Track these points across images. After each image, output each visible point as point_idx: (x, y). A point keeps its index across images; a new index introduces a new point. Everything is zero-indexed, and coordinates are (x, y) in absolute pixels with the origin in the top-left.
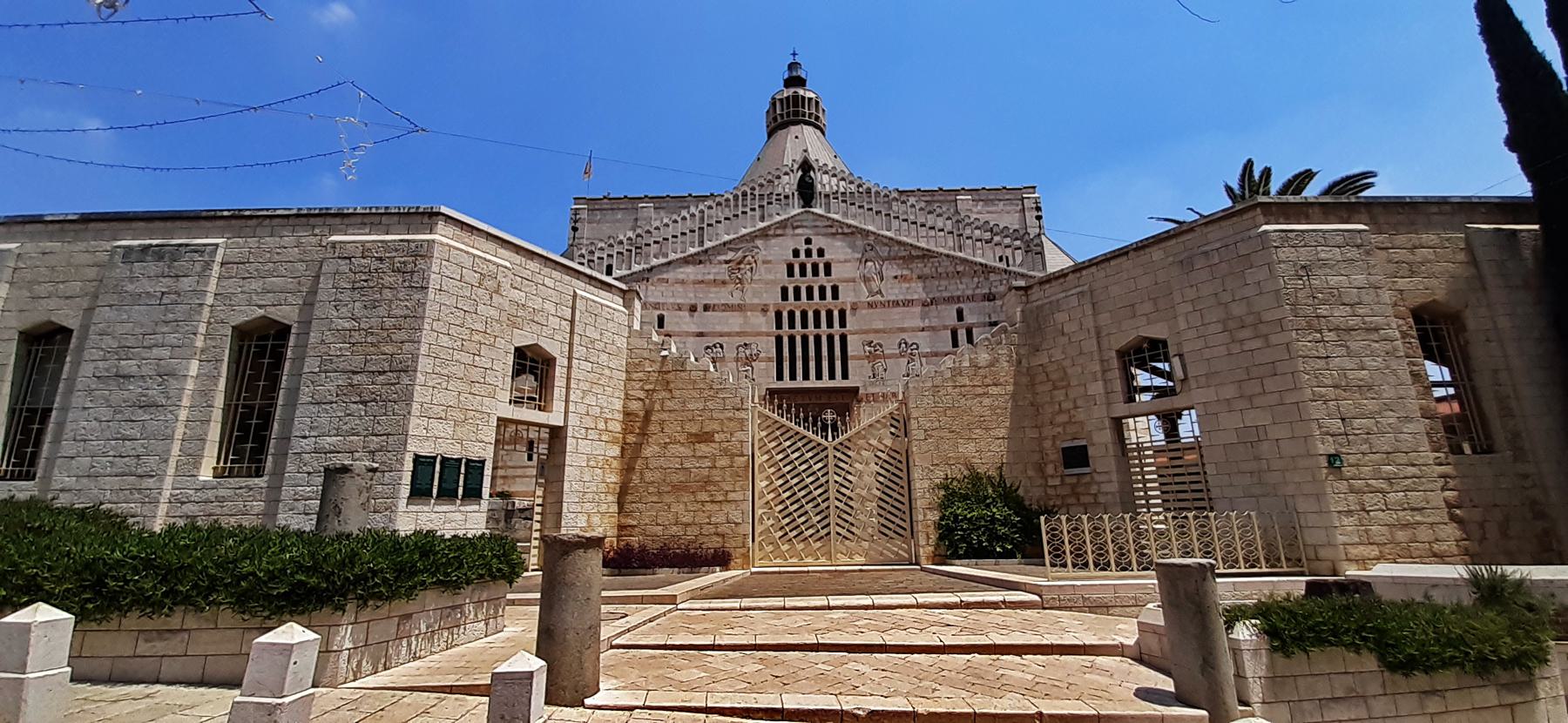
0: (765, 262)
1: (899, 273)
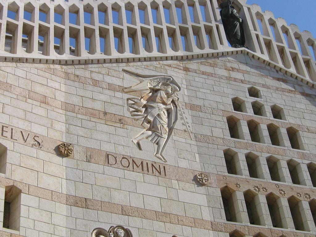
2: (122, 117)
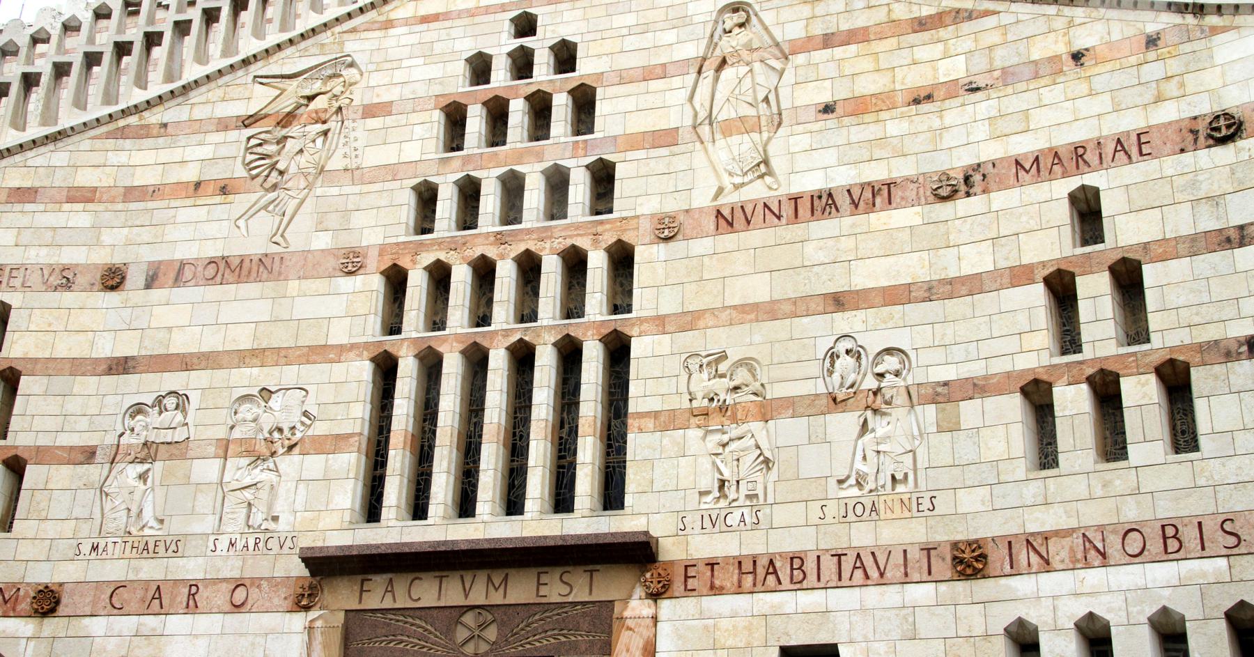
0: (370, 111)
1: (841, 94)
2: (226, 182)
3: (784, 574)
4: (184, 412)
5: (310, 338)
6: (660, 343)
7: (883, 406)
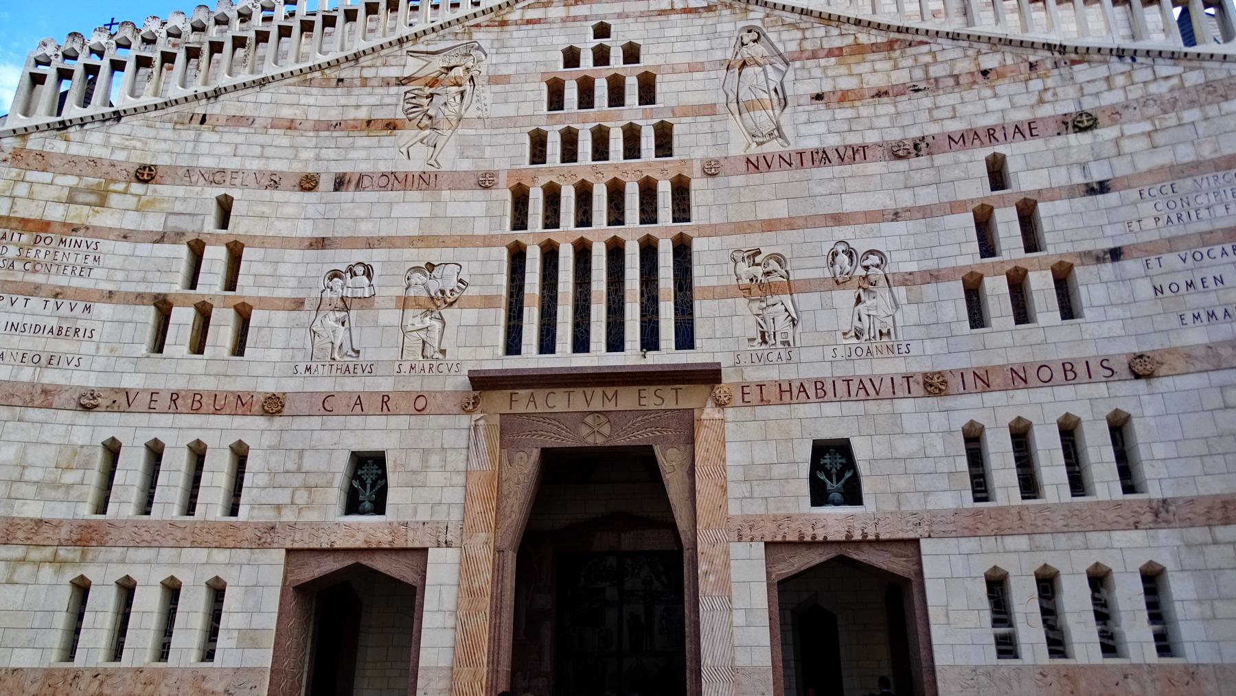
0: (494, 80)
1: (827, 87)
3: (811, 392)
4: (369, 276)
5: (459, 230)
6: (713, 242)
7: (870, 286)
